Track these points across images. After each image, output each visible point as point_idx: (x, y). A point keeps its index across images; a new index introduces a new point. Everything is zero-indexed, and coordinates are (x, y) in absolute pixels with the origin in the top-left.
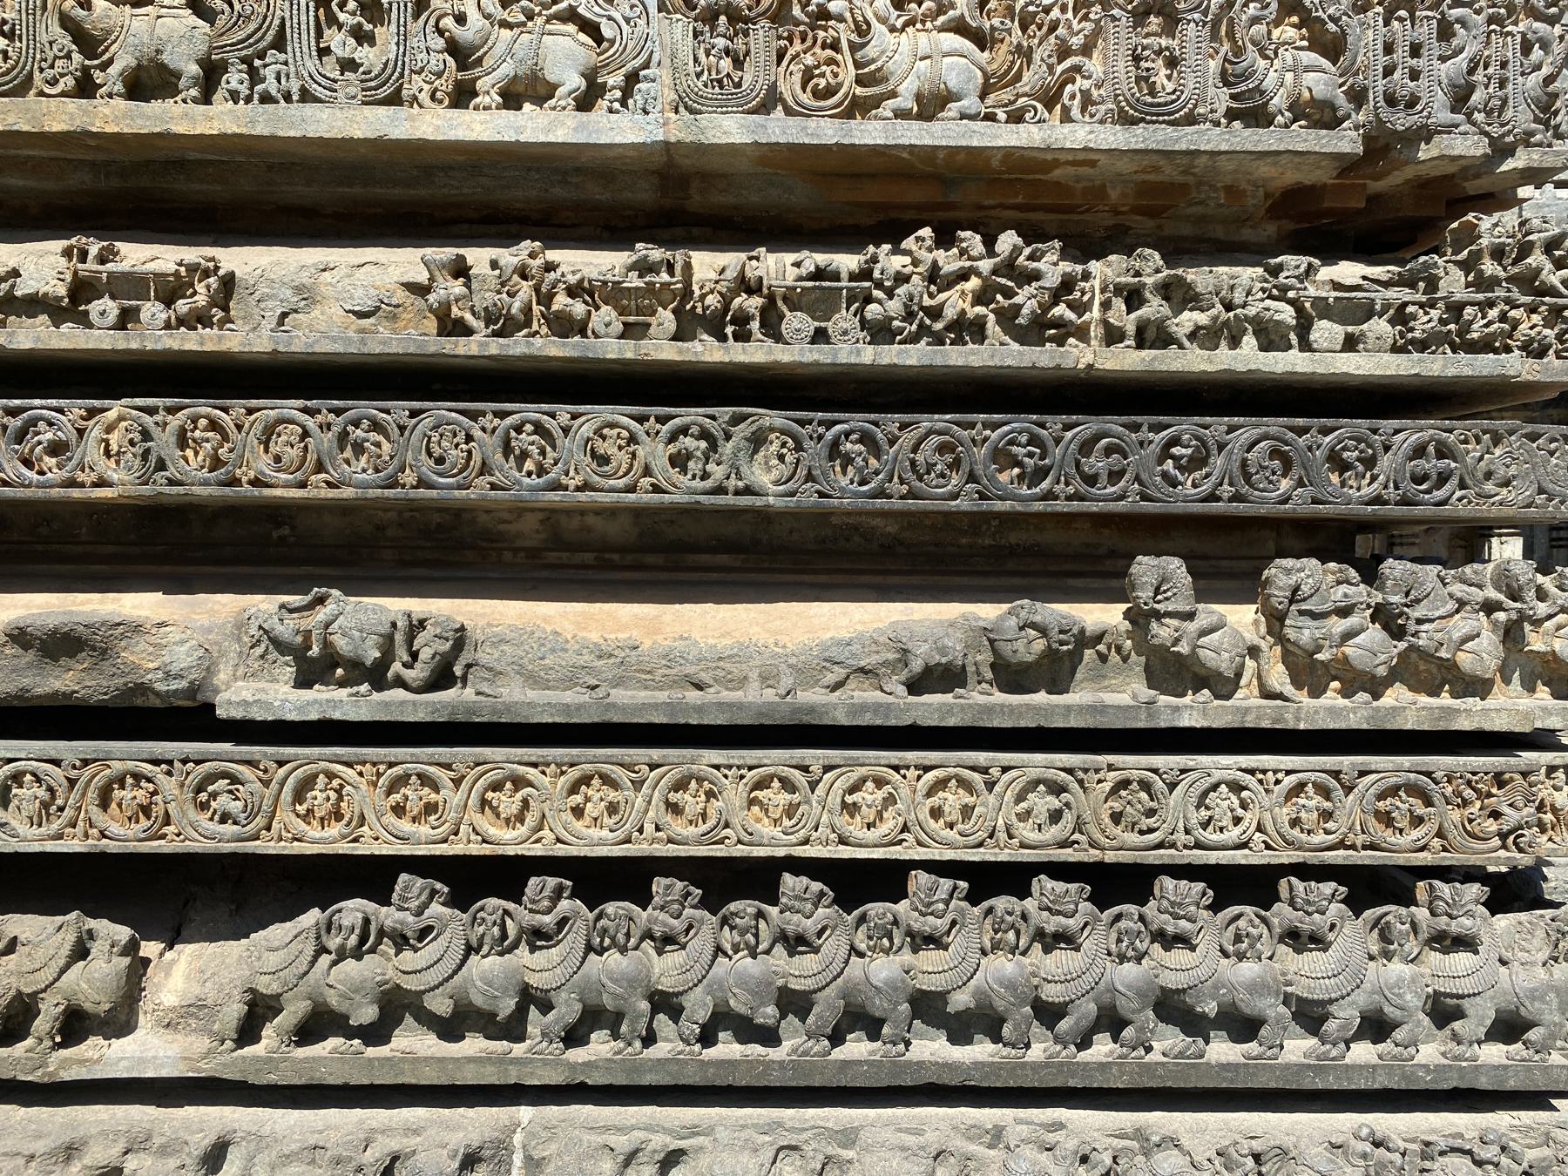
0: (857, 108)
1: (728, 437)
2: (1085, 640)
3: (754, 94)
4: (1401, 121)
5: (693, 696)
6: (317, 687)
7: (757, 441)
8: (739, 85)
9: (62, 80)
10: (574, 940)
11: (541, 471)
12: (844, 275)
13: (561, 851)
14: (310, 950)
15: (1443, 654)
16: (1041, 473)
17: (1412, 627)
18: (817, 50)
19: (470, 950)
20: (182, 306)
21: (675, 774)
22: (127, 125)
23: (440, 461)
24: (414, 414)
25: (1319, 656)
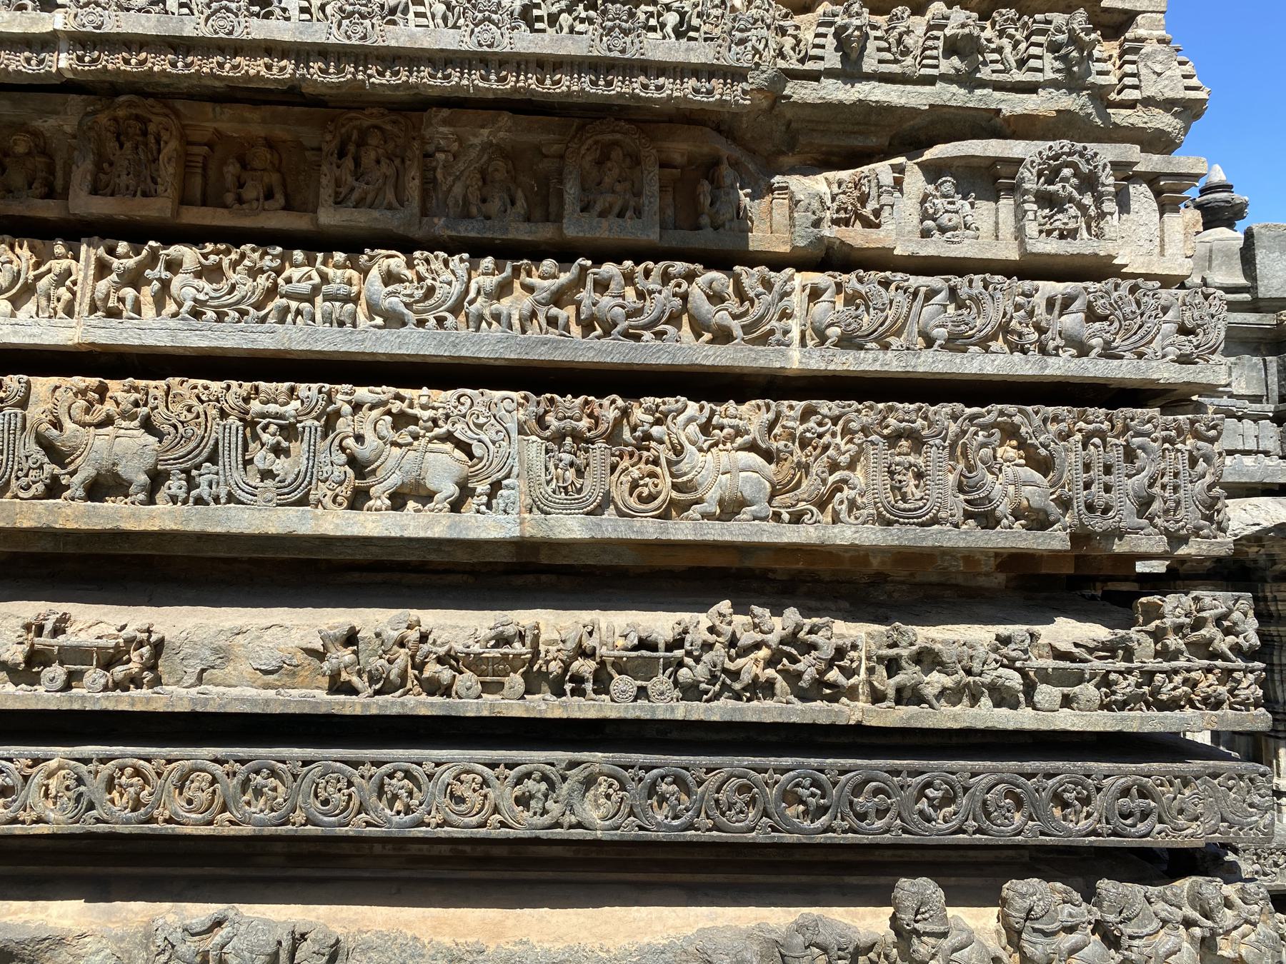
1: (564, 779)
3: (592, 499)
4: (1097, 524)
7: (589, 782)
8: (579, 491)
9: (34, 486)
11: (408, 810)
12: (662, 646)
16: (823, 810)
17: (1125, 942)
18: (642, 465)
20: (119, 671)
22: (85, 523)
23: (326, 802)
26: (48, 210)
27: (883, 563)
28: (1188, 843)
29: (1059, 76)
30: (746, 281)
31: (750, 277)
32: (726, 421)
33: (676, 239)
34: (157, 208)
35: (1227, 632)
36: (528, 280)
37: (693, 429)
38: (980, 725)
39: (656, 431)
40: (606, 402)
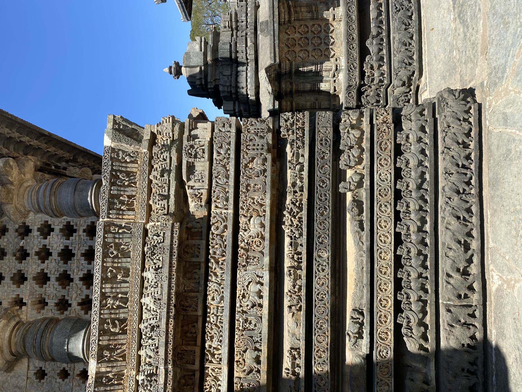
0: (263, 238)
1: (319, 262)
2: (354, 200)
4: (266, 147)
5: (364, 269)
6: (363, 335)
7: (320, 256)
8: (259, 258)
10: (409, 291)
11: (325, 294)
12: (291, 241)
13: (393, 293)
14: (411, 338)
15: (357, 140)
16: (325, 208)
19: (411, 310)
20: (297, 356)
21: (379, 273)
23: (324, 312)
24: (315, 316)
25: (357, 161)
26: (198, 375)
27: (274, 191)
28: (332, 131)
29: (168, 152)
30: (214, 222)
31: (213, 221)
32: (244, 226)
33: (204, 236)
34: (198, 350)
35: (289, 119)
36: (213, 269)
37: (245, 233)
38: (307, 174)
39: (246, 241)
40: (240, 252)
